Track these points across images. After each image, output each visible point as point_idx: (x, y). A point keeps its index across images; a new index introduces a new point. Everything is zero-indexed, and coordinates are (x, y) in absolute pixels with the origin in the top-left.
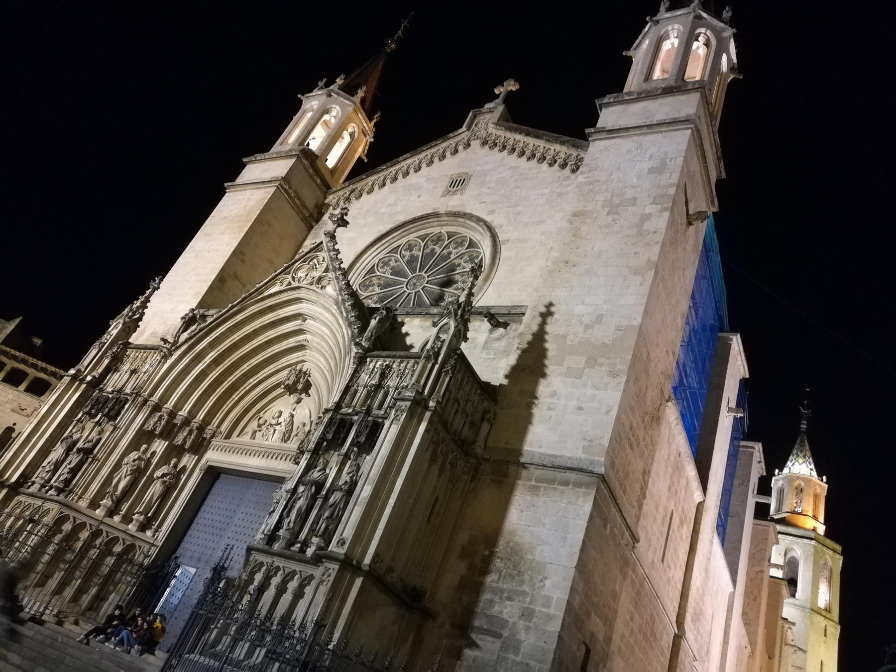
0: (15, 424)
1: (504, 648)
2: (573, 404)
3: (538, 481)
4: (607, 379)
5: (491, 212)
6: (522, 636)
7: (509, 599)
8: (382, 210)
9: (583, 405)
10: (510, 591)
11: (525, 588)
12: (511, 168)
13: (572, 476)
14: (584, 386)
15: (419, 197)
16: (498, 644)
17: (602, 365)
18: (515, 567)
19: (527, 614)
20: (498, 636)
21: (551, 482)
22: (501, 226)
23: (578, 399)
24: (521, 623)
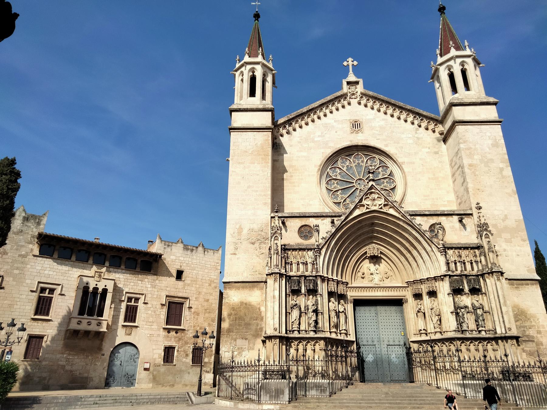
0: (106, 286)
1: (537, 344)
2: (514, 254)
3: (517, 285)
4: (522, 243)
5: (386, 146)
6: (541, 340)
7: (530, 328)
8: (316, 139)
9: (519, 254)
10: (529, 326)
11: (533, 323)
12: (383, 120)
13: (529, 282)
14: (515, 246)
15: (336, 132)
16: (534, 344)
17: (517, 237)
18: (526, 317)
19: (539, 332)
20: (534, 341)
21: (522, 285)
22: (396, 154)
23: (515, 251)
24: (539, 335)
